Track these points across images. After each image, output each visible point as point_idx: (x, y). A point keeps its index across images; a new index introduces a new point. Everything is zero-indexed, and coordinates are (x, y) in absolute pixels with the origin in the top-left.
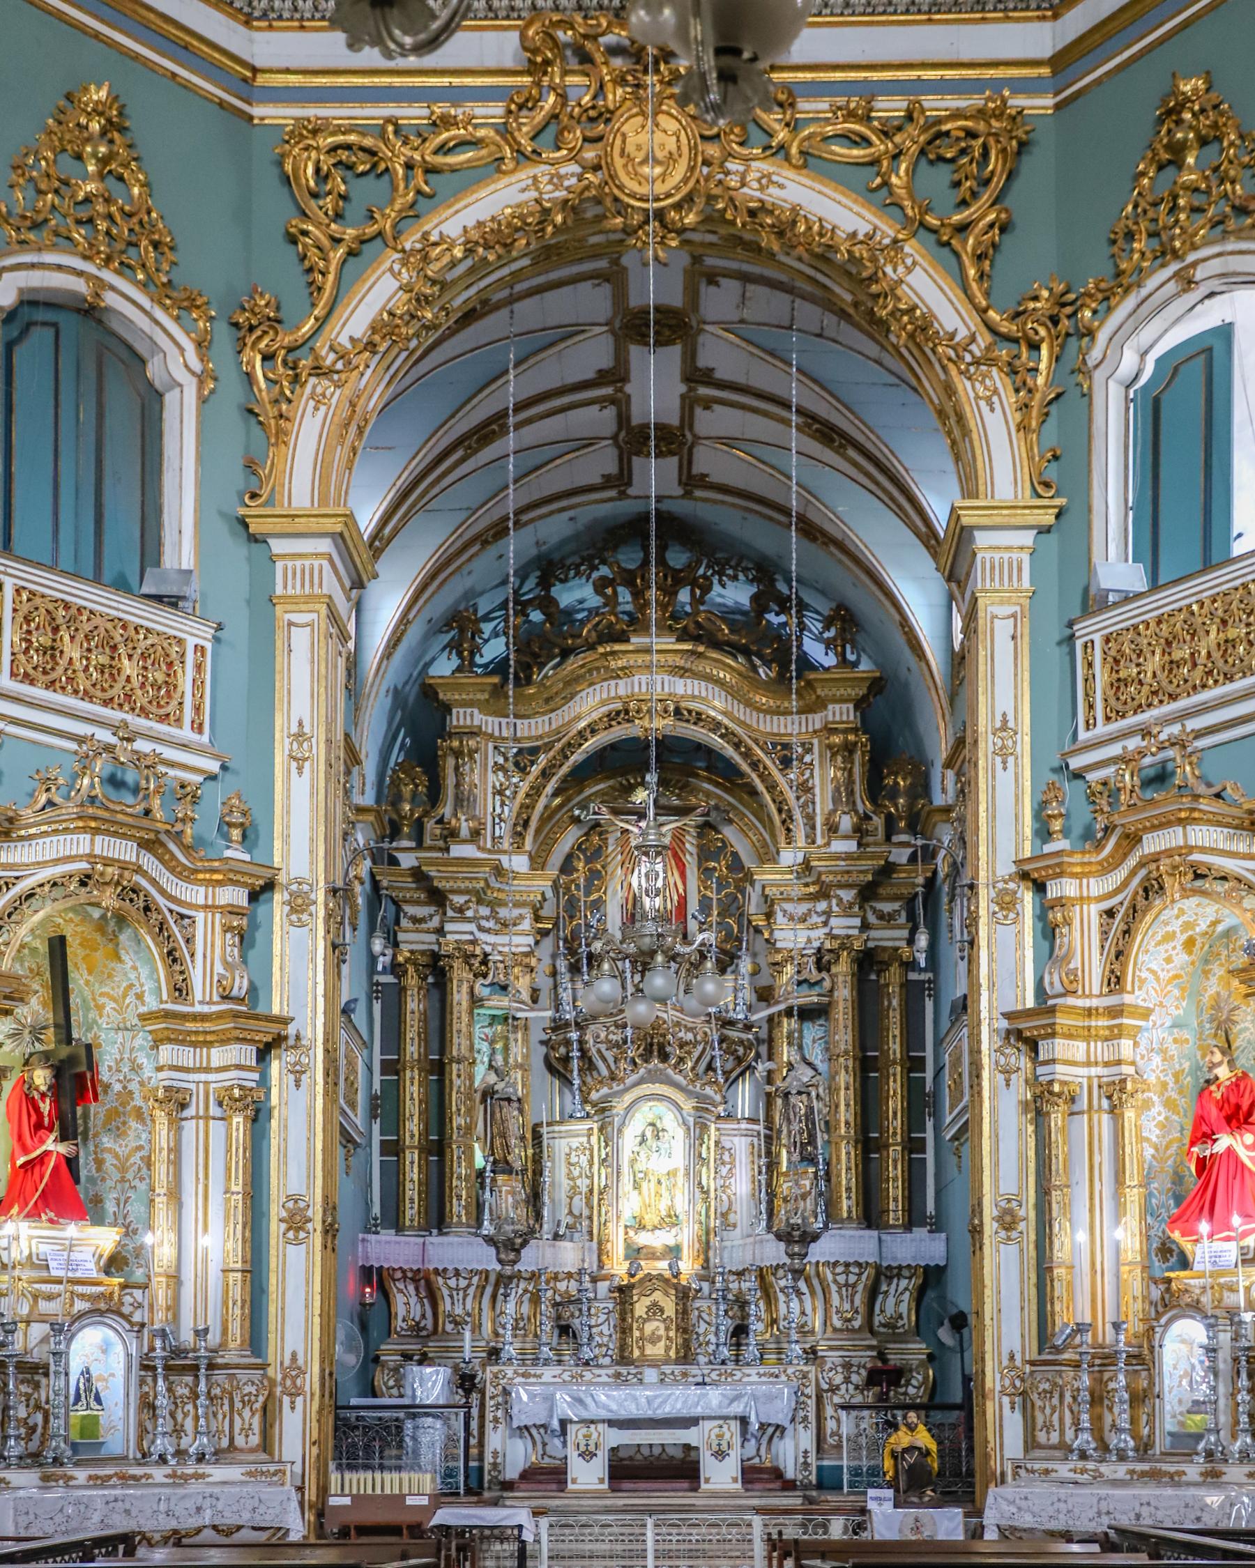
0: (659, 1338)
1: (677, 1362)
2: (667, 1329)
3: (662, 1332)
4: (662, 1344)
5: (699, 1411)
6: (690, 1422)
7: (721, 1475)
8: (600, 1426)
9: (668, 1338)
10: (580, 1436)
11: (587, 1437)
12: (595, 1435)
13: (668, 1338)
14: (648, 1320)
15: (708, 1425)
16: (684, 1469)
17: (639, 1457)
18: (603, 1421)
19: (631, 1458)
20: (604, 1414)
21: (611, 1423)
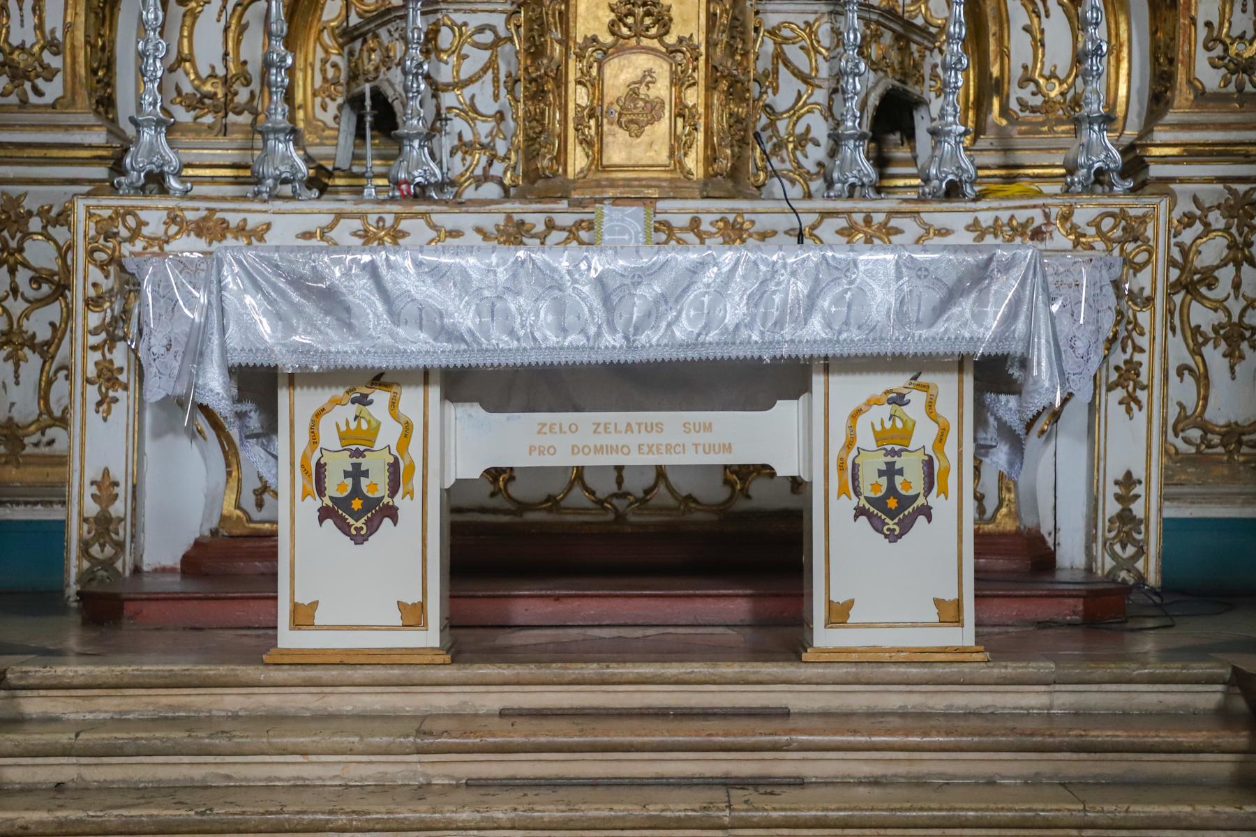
0: (653, 110)
1: (708, 189)
2: (679, 81)
3: (661, 89)
4: (663, 127)
5: (814, 334)
6: (784, 378)
7: (889, 591)
8: (411, 399)
9: (682, 111)
10: (329, 438)
11: (357, 443)
12: (389, 434)
13: (682, 111)
14: (617, 49)
15: (847, 391)
16: (748, 549)
17: (578, 497)
18: (425, 376)
19: (552, 502)
20: (419, 347)
21: (458, 383)
